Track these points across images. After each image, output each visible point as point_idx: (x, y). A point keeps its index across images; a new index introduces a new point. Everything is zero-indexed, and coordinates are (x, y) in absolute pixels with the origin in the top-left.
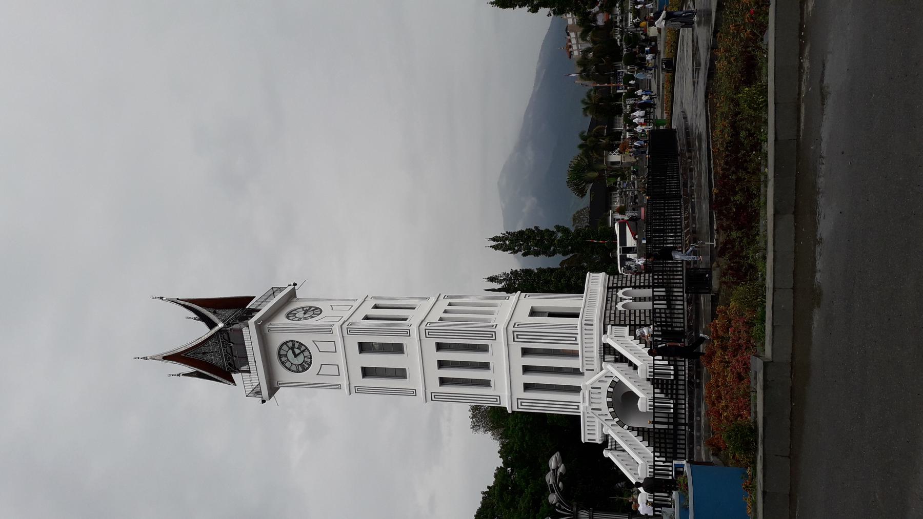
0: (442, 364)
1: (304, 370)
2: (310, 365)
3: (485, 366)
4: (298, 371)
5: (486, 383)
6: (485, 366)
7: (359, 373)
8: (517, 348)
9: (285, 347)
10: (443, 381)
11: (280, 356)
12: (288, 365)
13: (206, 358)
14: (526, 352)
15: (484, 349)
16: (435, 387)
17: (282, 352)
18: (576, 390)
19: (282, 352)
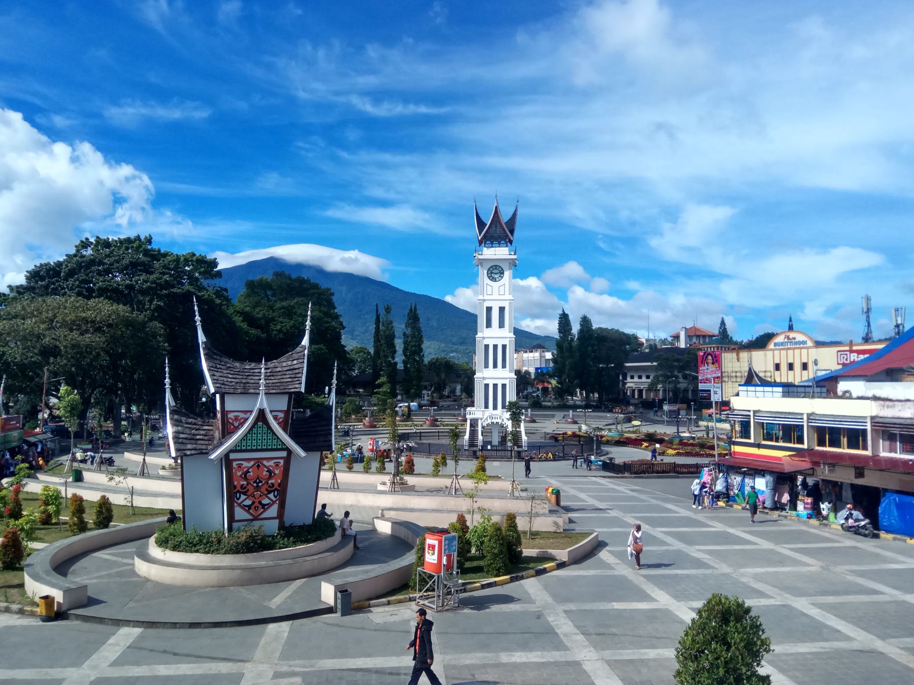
0: (495, 347)
1: (489, 277)
2: (491, 280)
3: (495, 366)
4: (488, 274)
5: (486, 366)
6: (495, 366)
7: (489, 305)
8: (507, 382)
9: (500, 269)
10: (487, 347)
11: (496, 266)
12: (491, 269)
13: (493, 226)
14: (504, 386)
15: (504, 366)
16: (486, 342)
17: (498, 267)
18: (486, 407)
19: (498, 267)
